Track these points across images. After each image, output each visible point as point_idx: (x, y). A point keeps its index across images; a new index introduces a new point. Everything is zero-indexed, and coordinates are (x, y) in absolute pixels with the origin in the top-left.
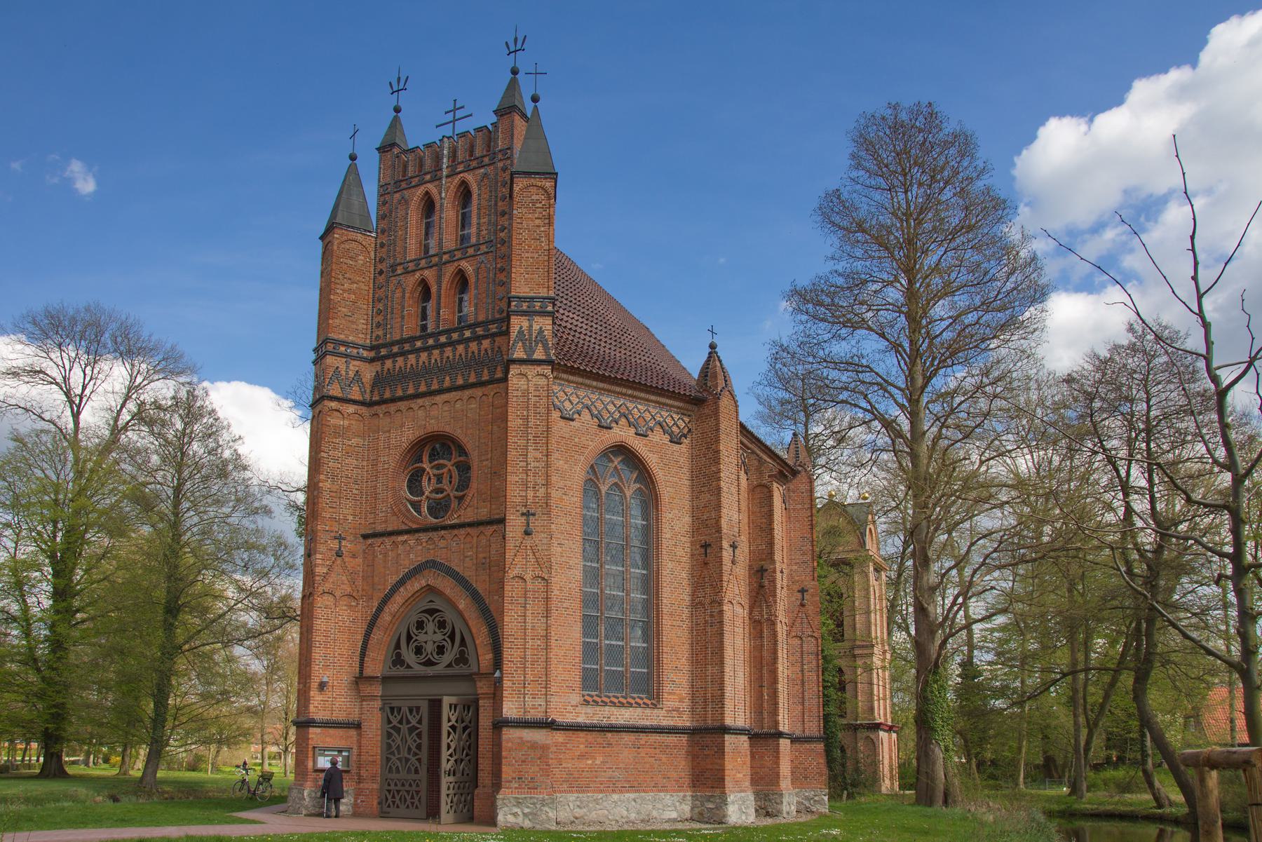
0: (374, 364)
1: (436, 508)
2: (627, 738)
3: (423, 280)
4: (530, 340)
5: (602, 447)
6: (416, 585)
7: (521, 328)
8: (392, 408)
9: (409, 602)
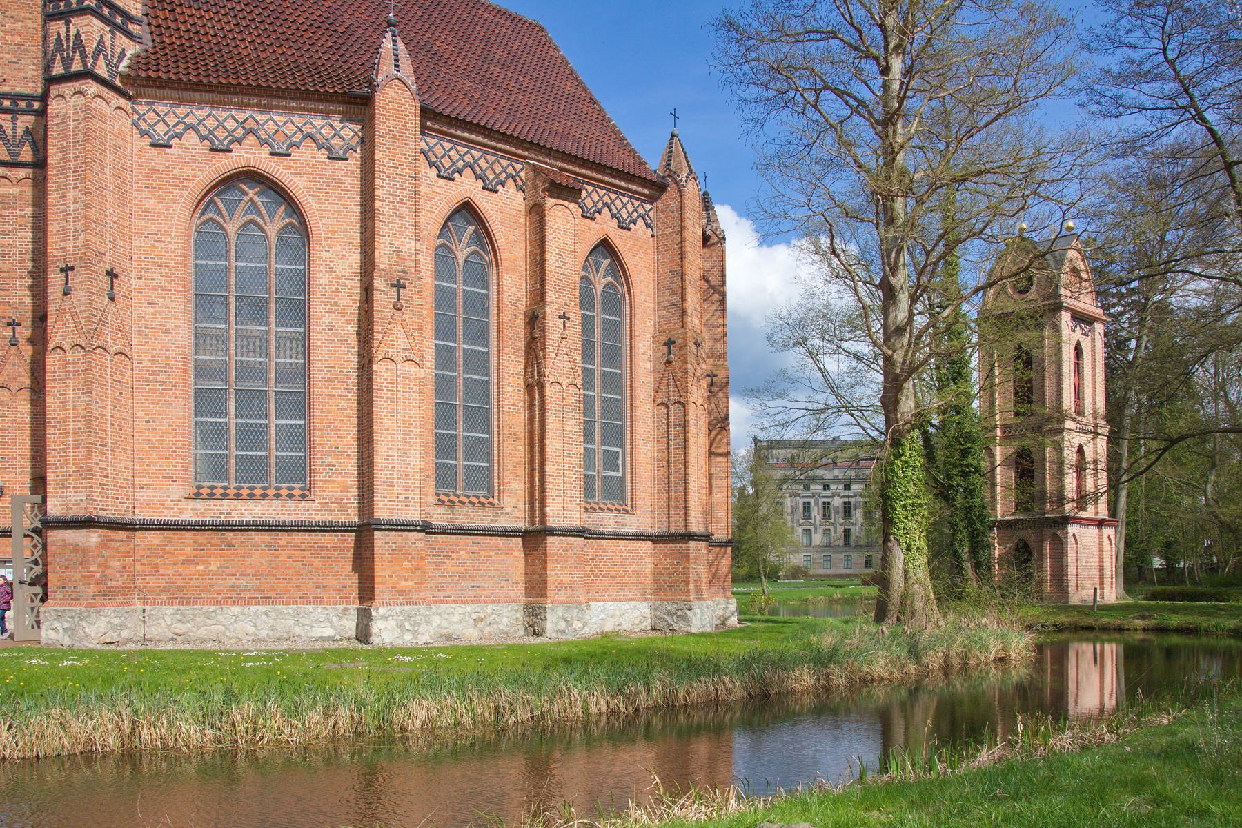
2: (257, 537)
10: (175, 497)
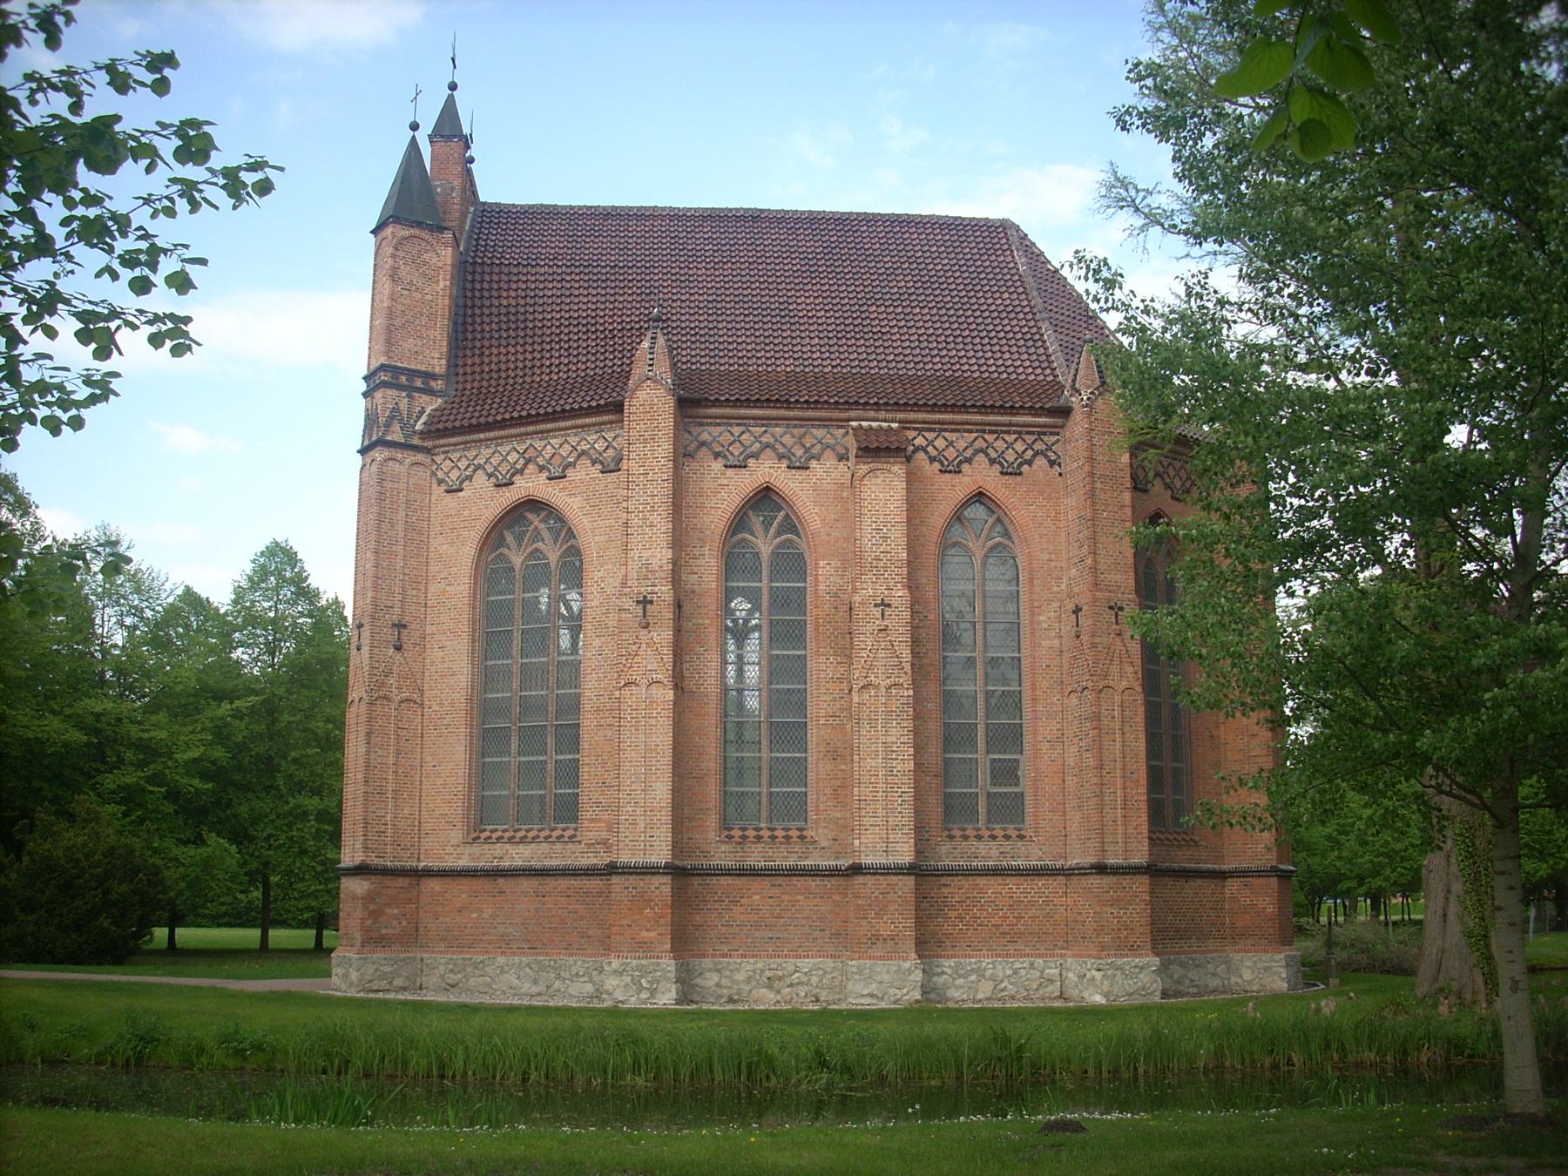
2: (527, 884)
10: (454, 842)
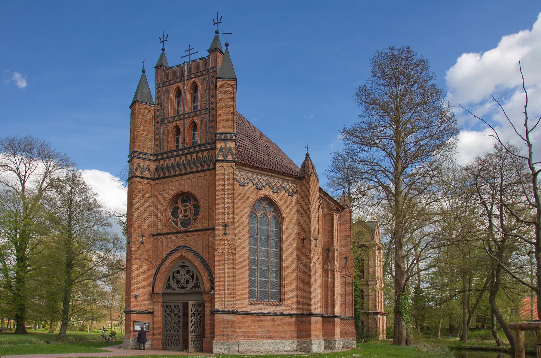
0: (156, 162)
1: (184, 223)
3: (177, 126)
4: (225, 151)
5: (258, 198)
6: (176, 255)
7: (221, 146)
8: (164, 181)
9: (173, 262)
10: (246, 304)
